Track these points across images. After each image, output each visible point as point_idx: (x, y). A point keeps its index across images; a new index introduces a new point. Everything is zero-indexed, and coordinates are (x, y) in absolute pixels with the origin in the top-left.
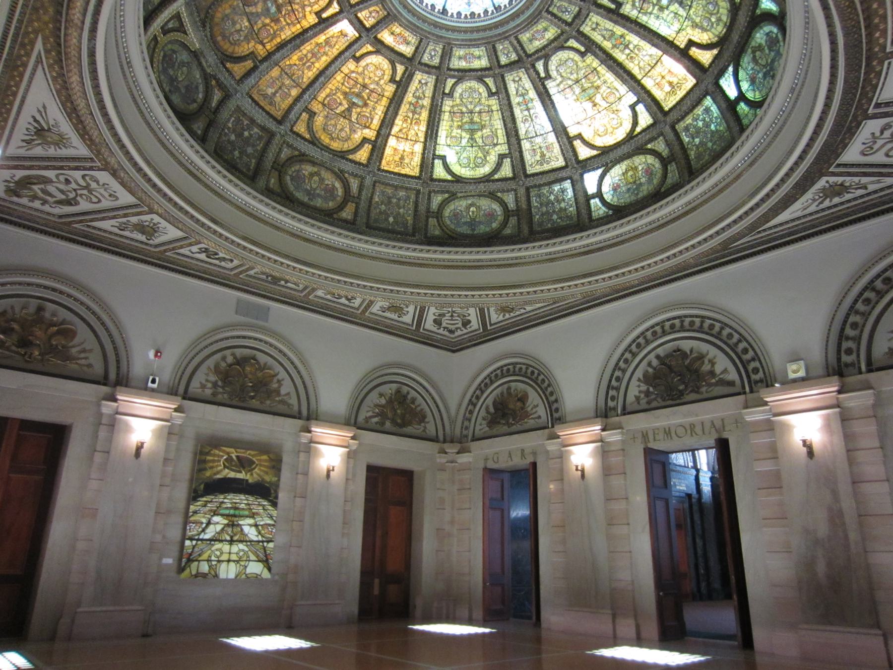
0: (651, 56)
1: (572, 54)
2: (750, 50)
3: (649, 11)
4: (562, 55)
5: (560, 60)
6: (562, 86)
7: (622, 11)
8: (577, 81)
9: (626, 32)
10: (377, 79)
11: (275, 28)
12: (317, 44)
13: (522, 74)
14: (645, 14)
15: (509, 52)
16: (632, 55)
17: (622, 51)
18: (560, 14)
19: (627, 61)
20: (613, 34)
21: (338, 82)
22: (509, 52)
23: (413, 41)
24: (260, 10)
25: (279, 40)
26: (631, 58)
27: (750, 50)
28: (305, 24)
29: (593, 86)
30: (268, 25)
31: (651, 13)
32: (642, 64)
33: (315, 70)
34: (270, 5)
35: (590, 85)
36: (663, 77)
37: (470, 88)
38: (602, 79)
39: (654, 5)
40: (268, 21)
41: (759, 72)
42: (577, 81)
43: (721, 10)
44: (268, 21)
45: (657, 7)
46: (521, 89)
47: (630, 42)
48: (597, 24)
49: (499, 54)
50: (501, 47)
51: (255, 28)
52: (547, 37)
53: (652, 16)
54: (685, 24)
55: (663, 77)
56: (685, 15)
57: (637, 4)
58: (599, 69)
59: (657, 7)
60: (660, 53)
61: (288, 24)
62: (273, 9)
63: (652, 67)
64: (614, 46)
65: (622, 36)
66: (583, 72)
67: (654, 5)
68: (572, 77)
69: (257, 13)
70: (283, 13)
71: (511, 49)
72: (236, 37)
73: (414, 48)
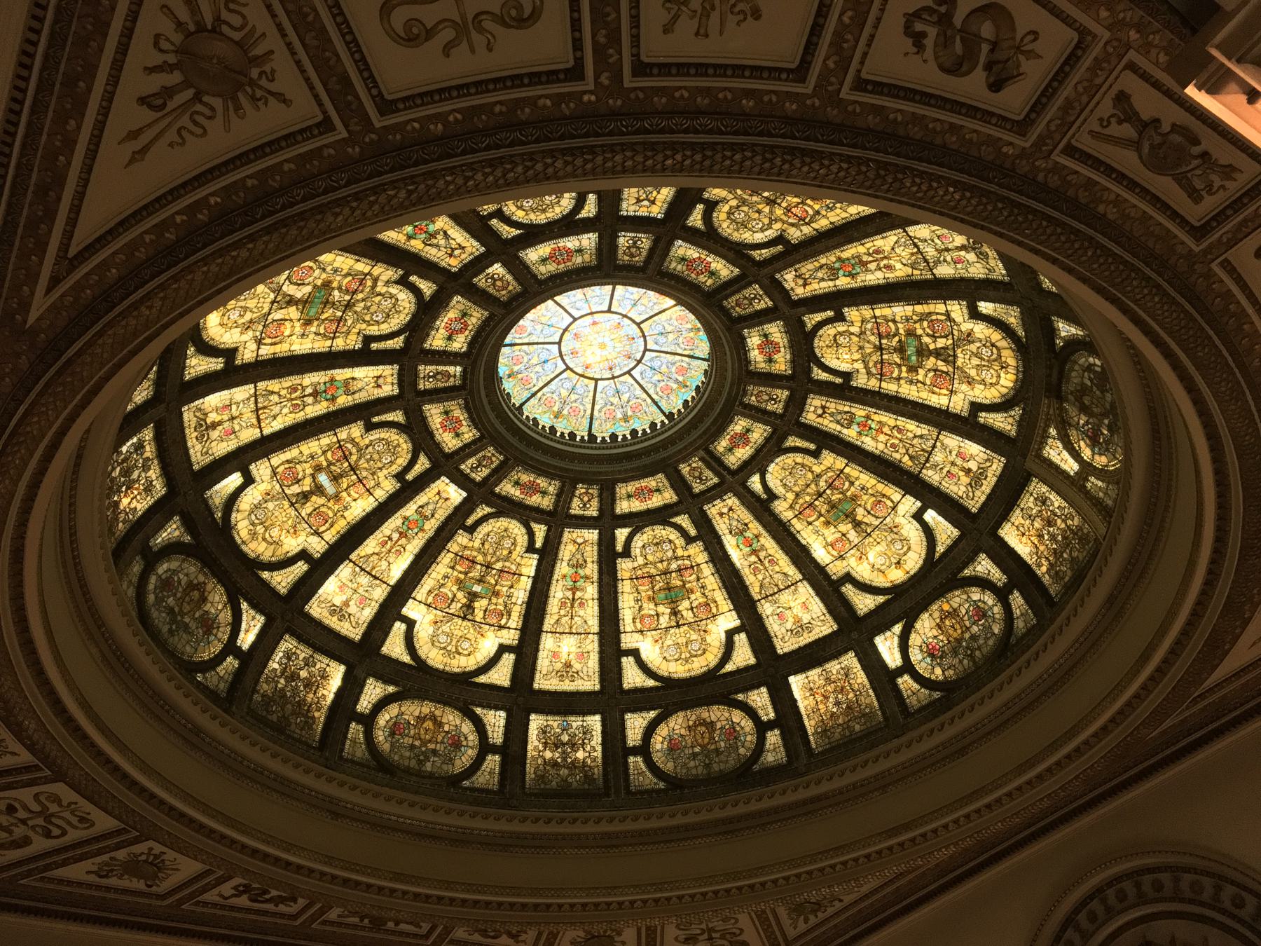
0: (275, 417)
1: (385, 328)
2: (201, 578)
3: (329, 453)
4: (396, 323)
5: (398, 312)
6: (369, 283)
7: (361, 423)
8: (349, 306)
9: (332, 408)
10: (745, 209)
11: (917, 325)
12: (853, 276)
13: (454, 264)
14: (330, 447)
15: (494, 284)
16: (298, 393)
17: (314, 385)
18: (441, 368)
19: (299, 382)
20: (347, 393)
21: (825, 217)
22: (494, 284)
23: (673, 265)
24: (932, 359)
25: (919, 308)
26: (295, 390)
27: (201, 578)
28: (866, 312)
29: (317, 319)
30: (928, 335)
31: (324, 452)
32: (275, 398)
33: (868, 245)
34: (914, 358)
35: (323, 317)
36: (233, 418)
37: (544, 211)
38: (312, 336)
39: (330, 464)
40: (926, 340)
41: (175, 595)
42: (349, 306)
43: (264, 544)
44: (926, 340)
45: (325, 464)
46: (442, 242)
47: (316, 402)
48: (379, 386)
49: (509, 277)
50: (510, 288)
51: (950, 342)
52: (442, 331)
53: (320, 452)
54: (278, 486)
55: (233, 418)
56: (287, 491)
57: (349, 446)
58: (328, 343)
59: (325, 464)
60: (267, 431)
61: (894, 321)
62: (911, 350)
63: (257, 410)
64: (332, 380)
65: (334, 399)
66: (349, 322)
67: (330, 464)
68: (362, 305)
69: (937, 358)
70: (897, 339)
71: (491, 290)
72: (986, 352)
73: (672, 253)
